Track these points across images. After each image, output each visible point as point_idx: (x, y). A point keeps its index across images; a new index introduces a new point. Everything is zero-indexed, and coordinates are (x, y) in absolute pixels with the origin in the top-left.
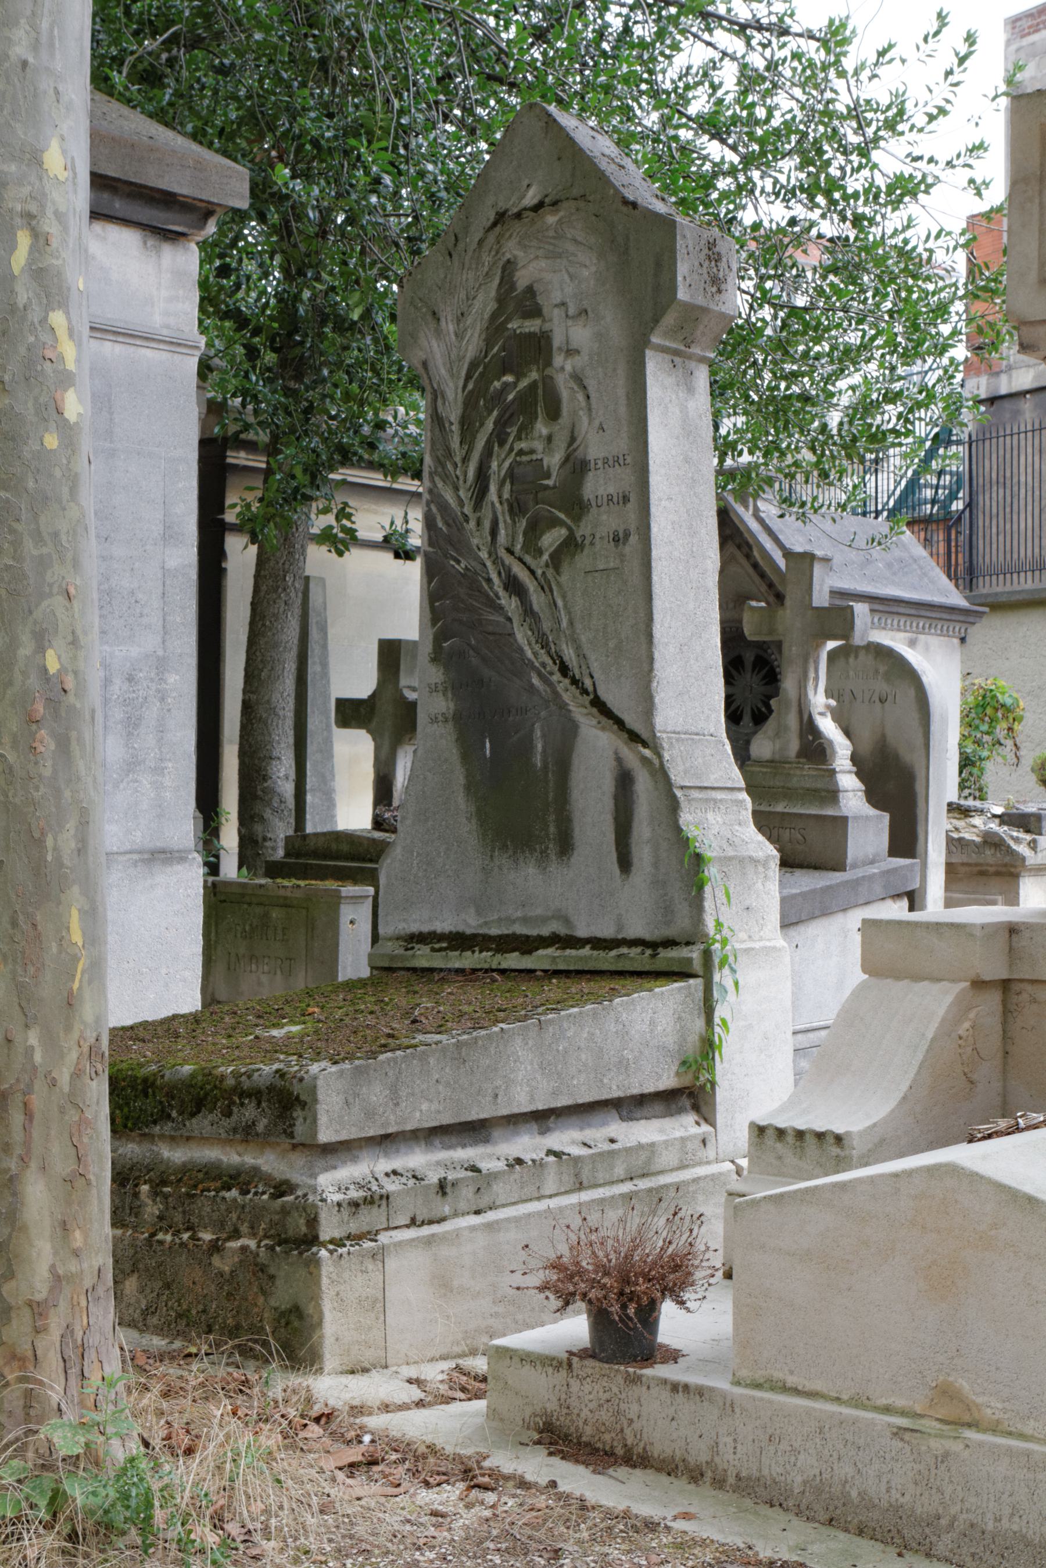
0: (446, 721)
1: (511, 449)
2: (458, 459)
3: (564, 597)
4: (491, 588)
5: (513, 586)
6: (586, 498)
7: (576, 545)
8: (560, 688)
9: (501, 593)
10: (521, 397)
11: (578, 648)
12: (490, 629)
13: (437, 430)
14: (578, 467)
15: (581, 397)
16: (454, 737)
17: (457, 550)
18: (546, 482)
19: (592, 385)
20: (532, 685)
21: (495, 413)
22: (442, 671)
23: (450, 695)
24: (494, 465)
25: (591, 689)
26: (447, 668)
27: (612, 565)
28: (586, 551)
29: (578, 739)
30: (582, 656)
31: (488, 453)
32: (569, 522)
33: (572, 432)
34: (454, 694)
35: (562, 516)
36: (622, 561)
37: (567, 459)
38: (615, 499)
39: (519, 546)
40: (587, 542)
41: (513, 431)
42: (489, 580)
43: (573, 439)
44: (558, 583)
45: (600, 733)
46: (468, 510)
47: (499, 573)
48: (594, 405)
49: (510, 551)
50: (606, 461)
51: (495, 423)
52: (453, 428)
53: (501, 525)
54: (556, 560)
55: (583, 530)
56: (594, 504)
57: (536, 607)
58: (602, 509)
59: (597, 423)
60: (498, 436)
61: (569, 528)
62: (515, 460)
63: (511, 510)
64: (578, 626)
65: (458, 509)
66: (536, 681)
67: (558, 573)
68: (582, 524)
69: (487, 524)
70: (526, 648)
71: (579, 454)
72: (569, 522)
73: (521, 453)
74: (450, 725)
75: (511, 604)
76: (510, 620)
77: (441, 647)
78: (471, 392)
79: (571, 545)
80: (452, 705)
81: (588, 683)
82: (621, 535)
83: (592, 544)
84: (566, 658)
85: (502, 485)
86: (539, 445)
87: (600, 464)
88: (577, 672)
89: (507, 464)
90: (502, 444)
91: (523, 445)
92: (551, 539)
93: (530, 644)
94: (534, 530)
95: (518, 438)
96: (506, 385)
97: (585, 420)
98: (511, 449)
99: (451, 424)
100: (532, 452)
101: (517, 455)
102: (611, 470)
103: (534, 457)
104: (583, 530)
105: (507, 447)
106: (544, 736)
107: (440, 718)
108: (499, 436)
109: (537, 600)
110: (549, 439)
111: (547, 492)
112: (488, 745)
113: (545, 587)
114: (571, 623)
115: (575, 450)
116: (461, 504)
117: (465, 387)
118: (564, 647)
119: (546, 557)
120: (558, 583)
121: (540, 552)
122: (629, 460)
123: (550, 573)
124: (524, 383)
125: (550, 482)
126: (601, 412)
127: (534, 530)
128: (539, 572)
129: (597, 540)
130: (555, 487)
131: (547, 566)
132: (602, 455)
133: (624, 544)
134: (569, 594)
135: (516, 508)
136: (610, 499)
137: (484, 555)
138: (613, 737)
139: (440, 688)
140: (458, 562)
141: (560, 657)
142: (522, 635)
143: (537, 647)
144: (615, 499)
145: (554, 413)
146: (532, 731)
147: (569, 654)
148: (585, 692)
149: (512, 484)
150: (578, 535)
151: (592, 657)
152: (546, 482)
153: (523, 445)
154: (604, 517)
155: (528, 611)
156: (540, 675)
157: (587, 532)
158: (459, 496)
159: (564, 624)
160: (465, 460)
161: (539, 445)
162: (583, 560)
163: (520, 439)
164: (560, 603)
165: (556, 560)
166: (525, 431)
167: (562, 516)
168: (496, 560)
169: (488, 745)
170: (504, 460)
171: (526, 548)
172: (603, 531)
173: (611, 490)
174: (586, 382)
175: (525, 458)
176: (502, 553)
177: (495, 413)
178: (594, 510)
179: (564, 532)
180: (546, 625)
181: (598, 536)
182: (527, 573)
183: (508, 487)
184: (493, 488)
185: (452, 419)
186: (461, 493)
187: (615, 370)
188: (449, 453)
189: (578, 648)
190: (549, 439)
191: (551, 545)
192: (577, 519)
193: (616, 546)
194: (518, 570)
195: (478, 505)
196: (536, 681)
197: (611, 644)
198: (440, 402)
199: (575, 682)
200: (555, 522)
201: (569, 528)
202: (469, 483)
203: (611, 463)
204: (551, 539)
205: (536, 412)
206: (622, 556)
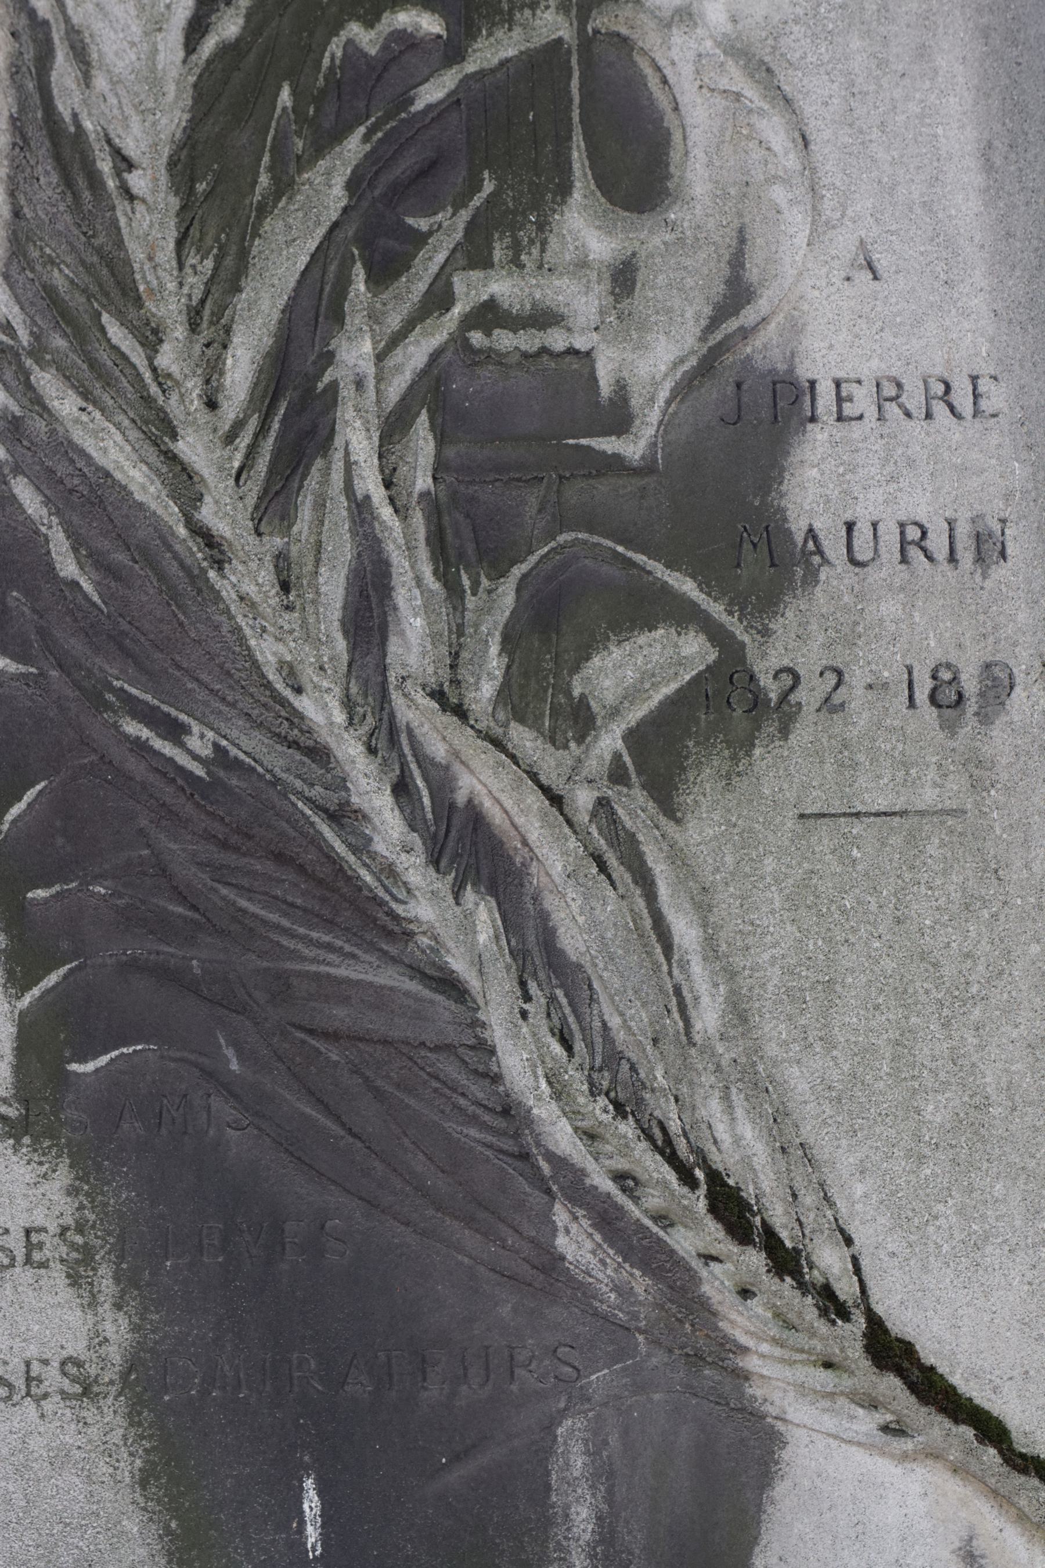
0: (88, 1390)
1: (439, 298)
2: (169, 309)
3: (703, 908)
4: (362, 847)
5: (469, 849)
6: (798, 527)
7: (757, 703)
8: (716, 1284)
9: (414, 869)
10: (477, 99)
11: (778, 1122)
12: (340, 1015)
13: (49, 177)
14: (755, 410)
15: (774, 131)
16: (129, 1467)
17: (152, 678)
18: (608, 445)
19: (818, 95)
20: (552, 1263)
21: (354, 147)
22: (63, 1176)
23: (107, 1285)
24: (356, 352)
25: (846, 1289)
26: (89, 1165)
27: (928, 796)
28: (802, 734)
29: (780, 1489)
30: (791, 1149)
31: (315, 311)
32: (716, 609)
33: (737, 262)
34: (128, 1281)
35: (689, 587)
36: (975, 785)
37: (707, 366)
38: (938, 543)
39: (488, 690)
40: (808, 697)
41: (445, 229)
42: (344, 816)
43: (737, 293)
44: (677, 856)
45: (884, 1468)
46: (224, 512)
47: (402, 789)
48: (830, 171)
49: (450, 702)
50: (889, 393)
51: (352, 186)
52: (137, 181)
53: (406, 597)
54: (661, 757)
55: (790, 645)
56: (834, 548)
57: (573, 942)
58: (874, 575)
59: (843, 243)
60: (366, 241)
61: (716, 634)
62: (459, 340)
63: (438, 542)
64: (773, 1031)
65: (170, 513)
66: (576, 1242)
67: (669, 808)
68: (786, 623)
69: (333, 586)
70: (545, 1111)
71: (765, 348)
72: (716, 609)
73: (489, 315)
74: (109, 1418)
75: (459, 928)
76: (450, 985)
77: (62, 1079)
78: (229, 51)
79: (728, 710)
80: (117, 1329)
81: (829, 1260)
82: (970, 685)
83: (829, 706)
84: (725, 1159)
85: (393, 429)
86: (582, 302)
87: (863, 401)
88: (779, 1217)
89: (416, 353)
90: (385, 271)
91: (502, 287)
92: (633, 673)
93: (559, 1093)
94: (552, 632)
95: (474, 254)
96: (406, 42)
97: (797, 222)
98: (439, 298)
99: (124, 163)
100: (544, 318)
101: (469, 322)
102: (917, 427)
103: (557, 340)
104: (790, 645)
105: (416, 285)
106: (603, 1474)
107: (53, 1378)
108: (373, 233)
109: (582, 917)
110: (624, 278)
111: (603, 487)
112: (311, 1504)
113: (617, 857)
114: (739, 1014)
115: (745, 333)
116: (183, 483)
117: (196, 30)
118: (713, 1108)
119: (610, 741)
120: (677, 856)
121: (580, 720)
122: (995, 398)
123: (635, 807)
124: (494, 50)
125: (632, 448)
126: (863, 204)
127: (552, 632)
128: (583, 799)
129: (855, 693)
130: (647, 468)
131: (617, 775)
132: (870, 368)
133: (985, 718)
134: (726, 900)
135: (465, 543)
136: (913, 541)
137: (322, 710)
138: (954, 1487)
139: (52, 1249)
140: (175, 732)
141: (704, 1162)
142: (521, 1057)
143: (600, 1110)
144: (938, 543)
145: (639, 179)
146: (543, 1447)
147: (739, 1142)
148: (831, 1305)
149: (441, 438)
150: (765, 666)
151: (843, 1160)
152: (608, 445)
153: (502, 287)
154: (890, 608)
155: (538, 956)
156: (607, 1220)
157: (809, 660)
158: (171, 458)
159: (708, 1017)
160: (210, 320)
161: (582, 302)
162: (788, 770)
163: (484, 262)
164: (685, 931)
165: (661, 757)
166: (511, 227)
167: (689, 587)
168: (387, 738)
169: (311, 1504)
170: (397, 339)
171: (514, 699)
172: (875, 661)
173: (919, 505)
174: (789, 81)
175: (505, 340)
176: (415, 711)
177: (354, 147)
178: (836, 576)
179: (695, 650)
180: (625, 1013)
181: (857, 677)
182: (535, 800)
183: (422, 442)
184: (357, 438)
185: (131, 147)
186: (192, 447)
187: (922, 53)
188: (120, 288)
189: (778, 1122)
190: (624, 278)
191: (632, 695)
192: (762, 601)
193: (950, 728)
194: (485, 783)
195: (274, 506)
196: (576, 1242)
197: (936, 1111)
198: (63, 70)
199: (786, 1261)
200: (646, 609)
201: (716, 634)
202: (231, 410)
203: (914, 400)
204: (633, 673)
205: (564, 168)
206: (977, 769)
